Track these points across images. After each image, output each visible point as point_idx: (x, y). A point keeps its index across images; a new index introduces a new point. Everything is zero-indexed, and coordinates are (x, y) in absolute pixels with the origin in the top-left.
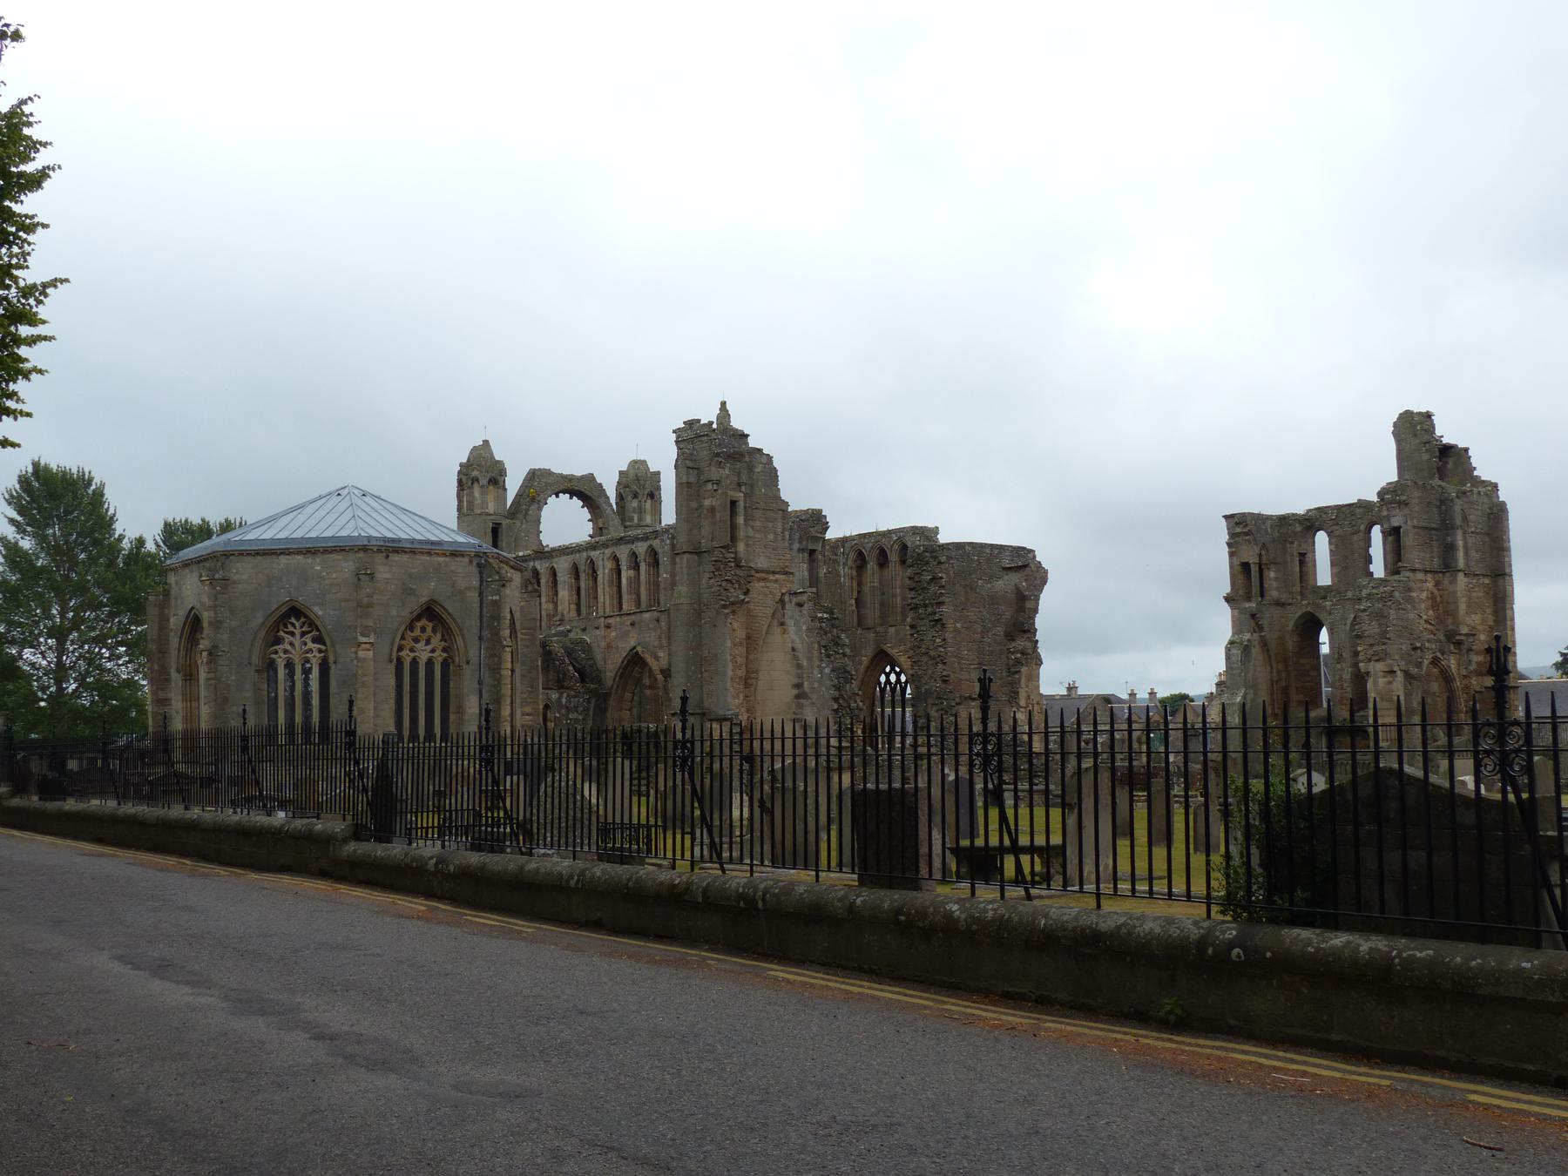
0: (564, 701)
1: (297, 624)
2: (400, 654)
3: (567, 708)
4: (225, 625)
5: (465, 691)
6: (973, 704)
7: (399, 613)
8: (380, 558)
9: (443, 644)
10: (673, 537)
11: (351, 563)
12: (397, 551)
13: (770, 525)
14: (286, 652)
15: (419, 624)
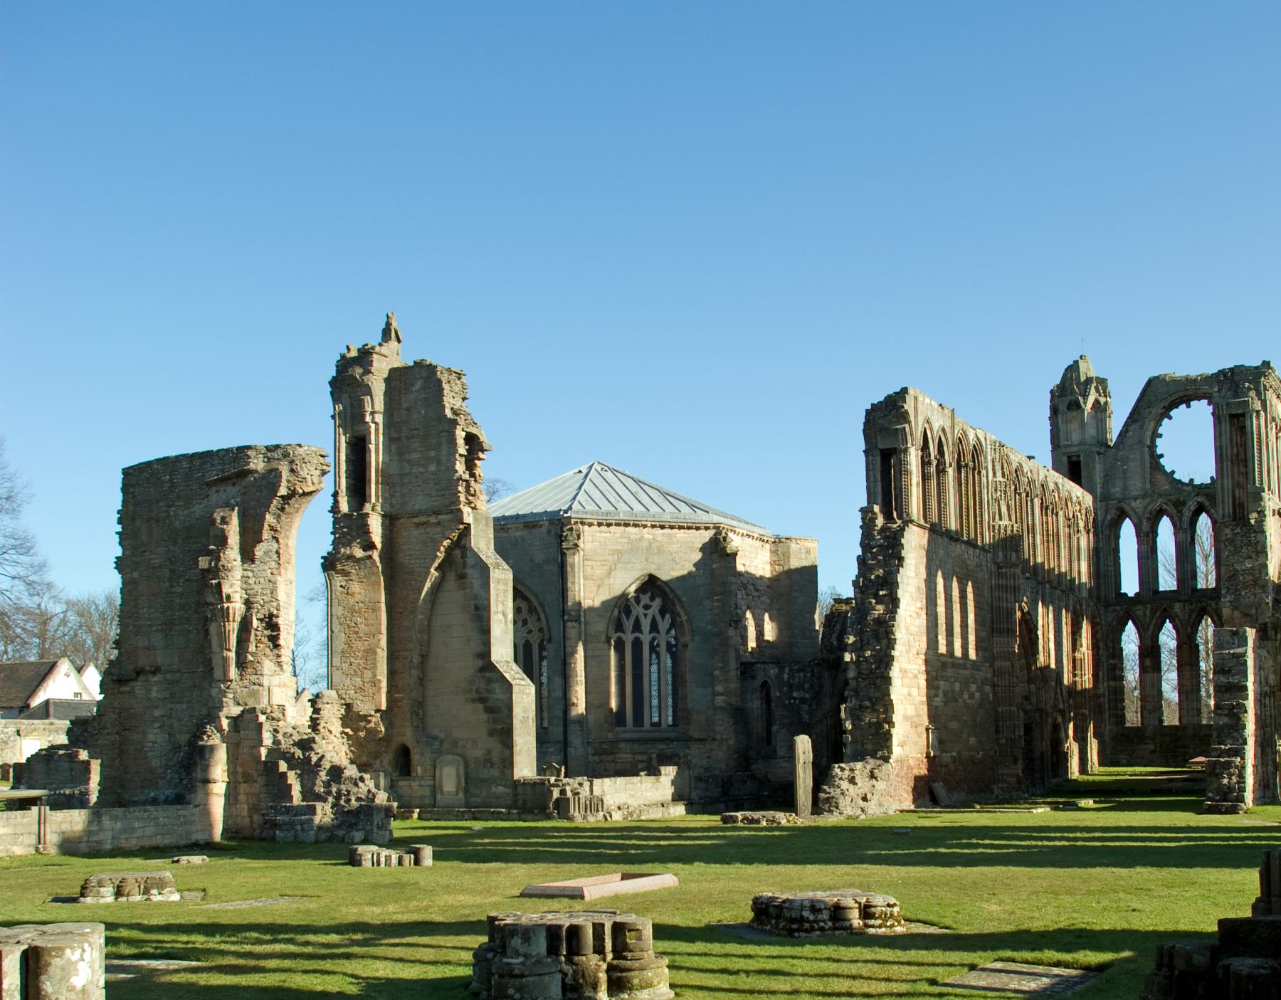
0: (786, 676)
3: (790, 686)
6: (155, 679)
13: (432, 454)
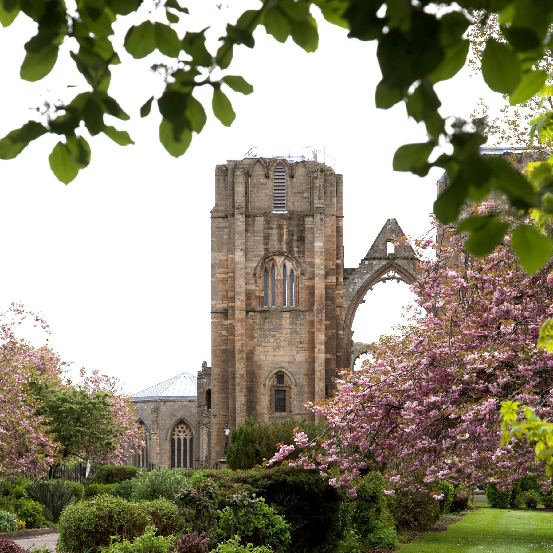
7: (170, 423)
8: (162, 404)
12: (168, 401)
15: (180, 426)
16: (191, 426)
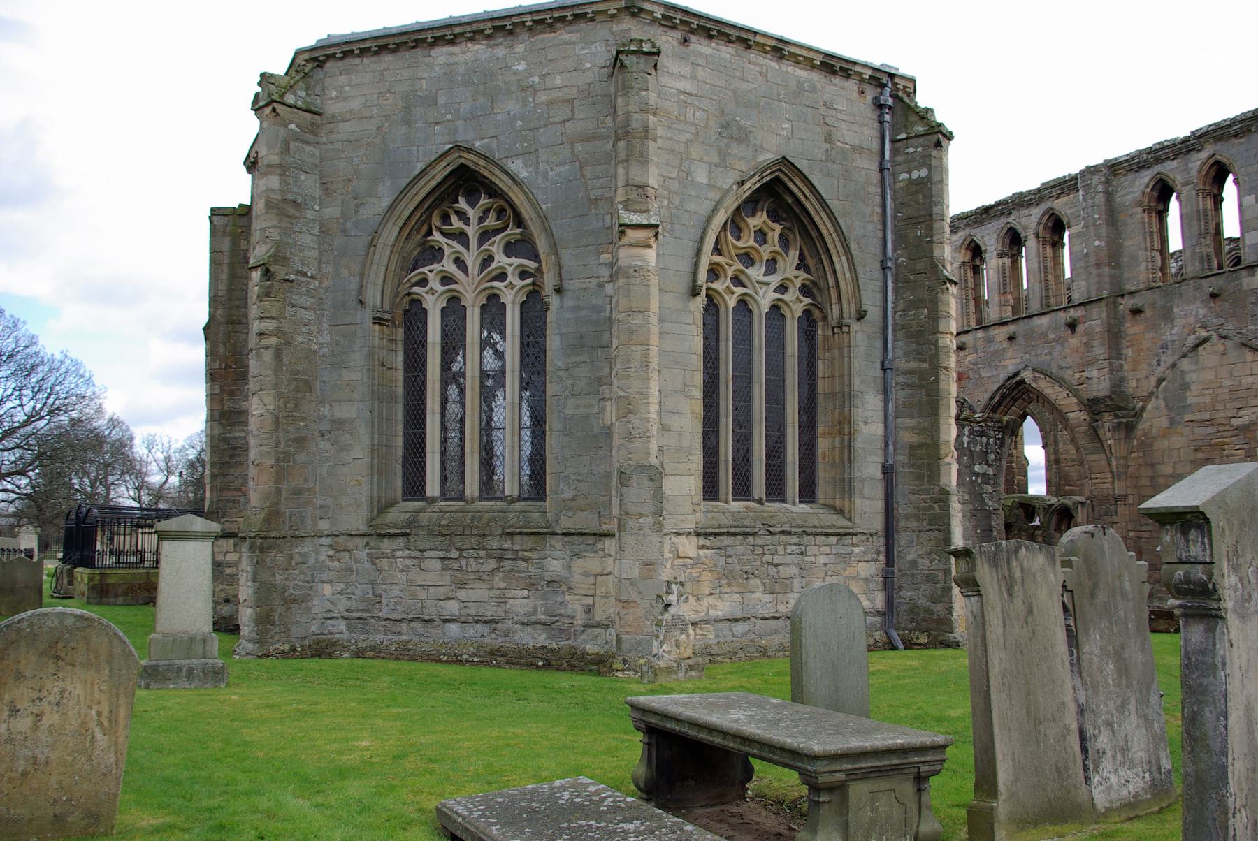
1: (472, 213)
2: (714, 285)
4: (310, 214)
5: (857, 383)
9: (803, 275)
10: (1108, 182)
11: (599, 47)
14: (446, 279)
16: (826, 228)
